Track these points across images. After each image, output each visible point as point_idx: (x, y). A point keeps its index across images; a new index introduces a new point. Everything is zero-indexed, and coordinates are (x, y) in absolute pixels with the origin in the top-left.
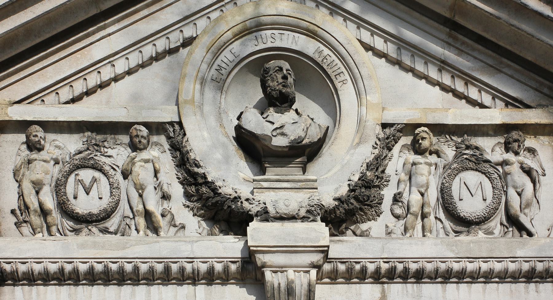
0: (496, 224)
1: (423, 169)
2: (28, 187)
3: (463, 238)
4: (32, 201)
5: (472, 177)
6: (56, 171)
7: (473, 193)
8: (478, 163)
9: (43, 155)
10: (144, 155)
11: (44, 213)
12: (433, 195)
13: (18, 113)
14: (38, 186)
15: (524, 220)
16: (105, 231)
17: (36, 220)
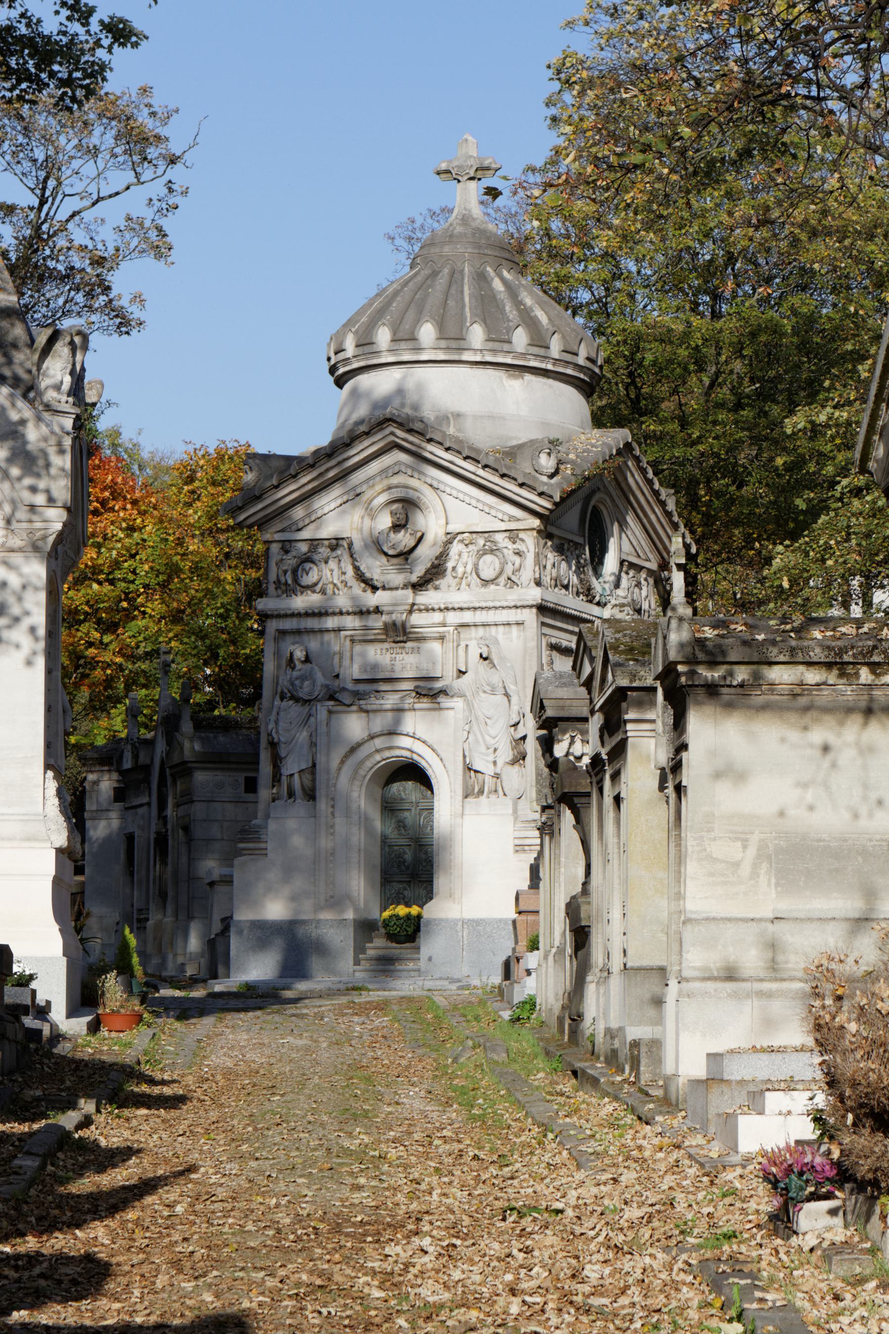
0: (502, 580)
1: (465, 556)
2: (280, 572)
3: (483, 590)
4: (283, 579)
5: (488, 558)
6: (294, 562)
7: (489, 566)
8: (493, 550)
9: (290, 556)
10: (334, 554)
11: (286, 584)
12: (470, 567)
13: (277, 537)
14: (285, 572)
15: (513, 578)
16: (314, 592)
17: (284, 588)
